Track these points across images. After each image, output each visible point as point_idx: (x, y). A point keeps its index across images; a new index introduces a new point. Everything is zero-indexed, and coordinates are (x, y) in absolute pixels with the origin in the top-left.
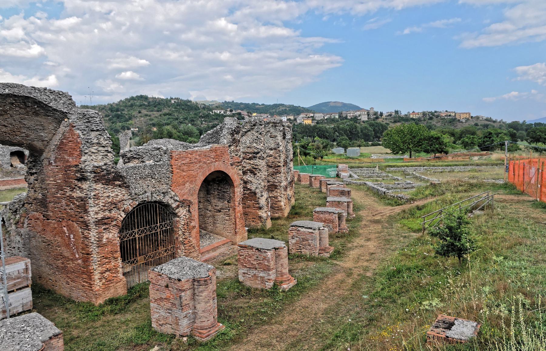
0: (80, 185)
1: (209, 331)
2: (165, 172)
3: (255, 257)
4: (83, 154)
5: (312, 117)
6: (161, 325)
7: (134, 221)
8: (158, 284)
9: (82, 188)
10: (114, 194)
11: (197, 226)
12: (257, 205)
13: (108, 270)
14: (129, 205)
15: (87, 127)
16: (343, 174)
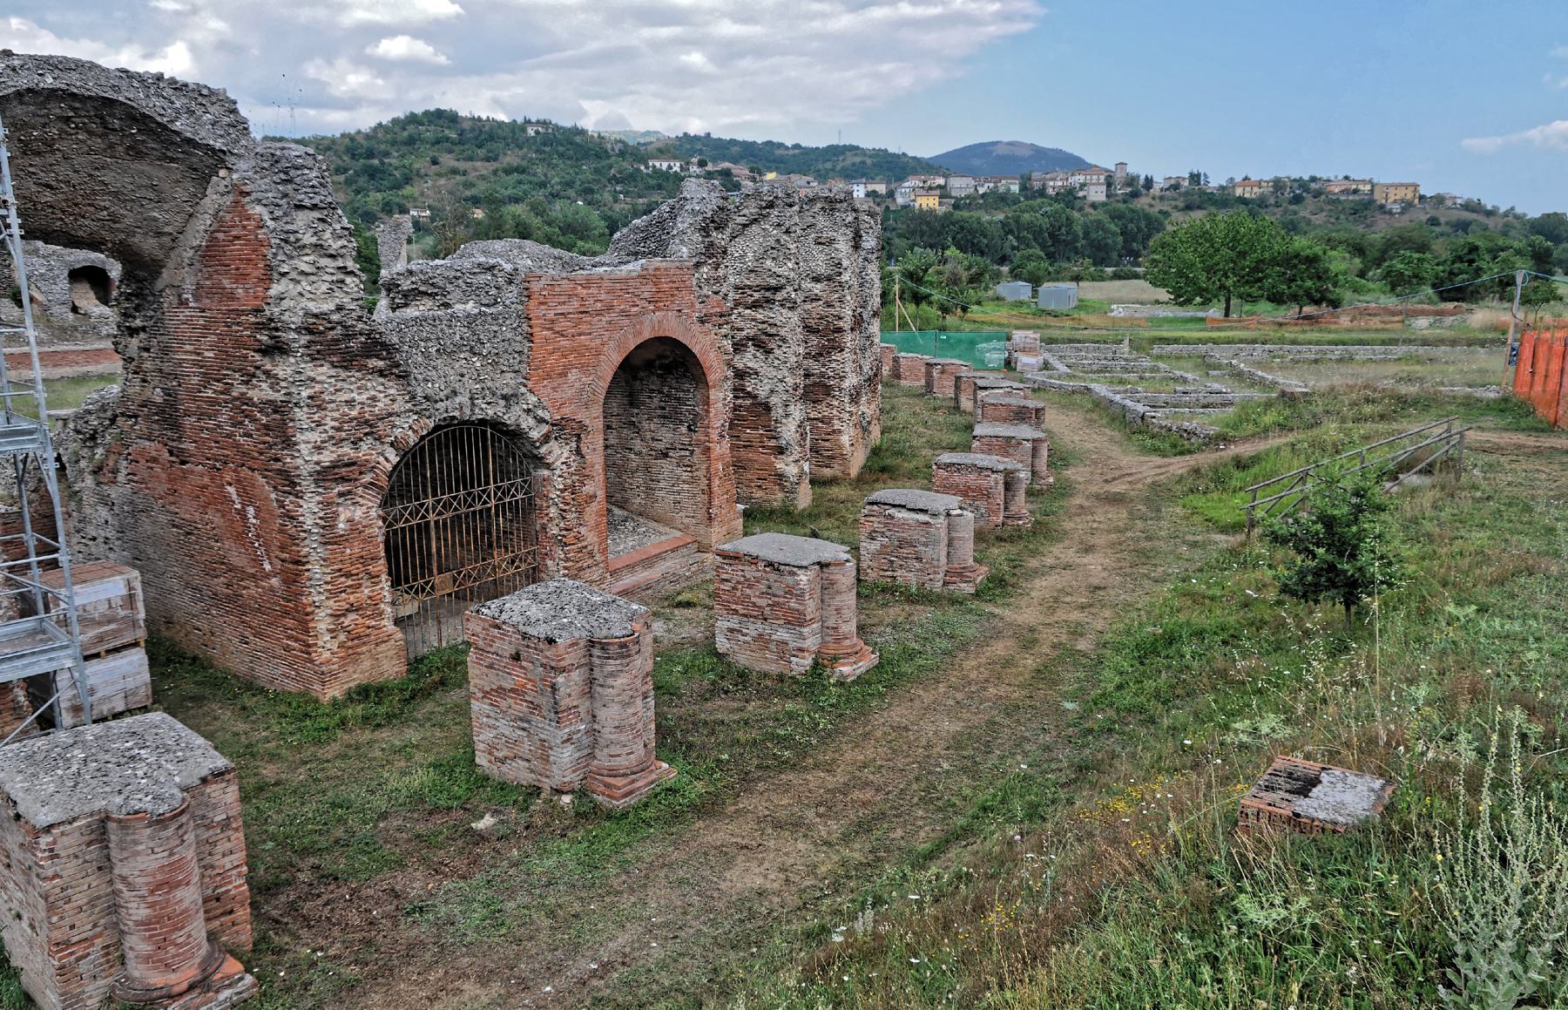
0: (268, 367)
1: (633, 781)
2: (509, 336)
3: (763, 588)
4: (276, 276)
5: (940, 187)
6: (503, 761)
7: (424, 476)
8: (492, 650)
9: (275, 377)
10: (365, 397)
11: (601, 494)
12: (773, 443)
13: (352, 609)
14: (409, 429)
15: (285, 195)
16: (1024, 360)
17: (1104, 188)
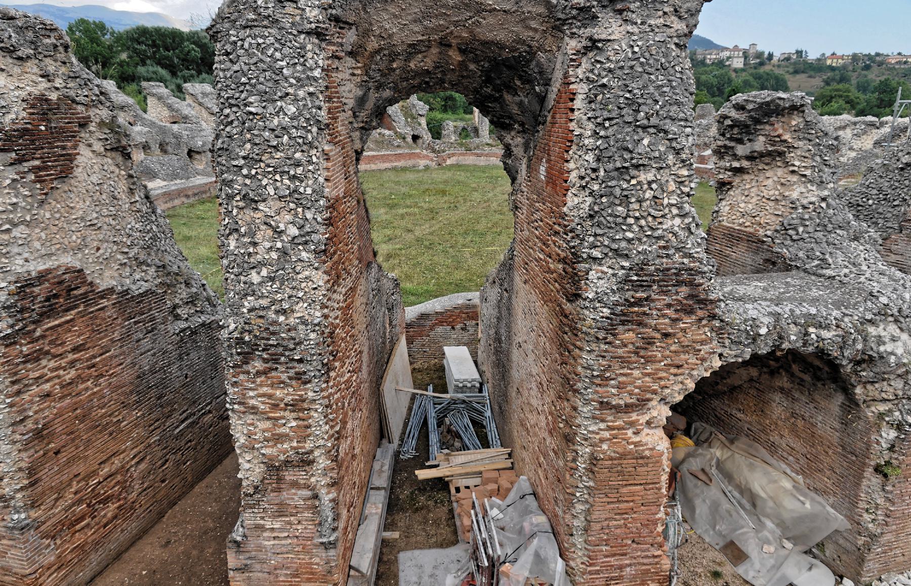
17: (742, 60)
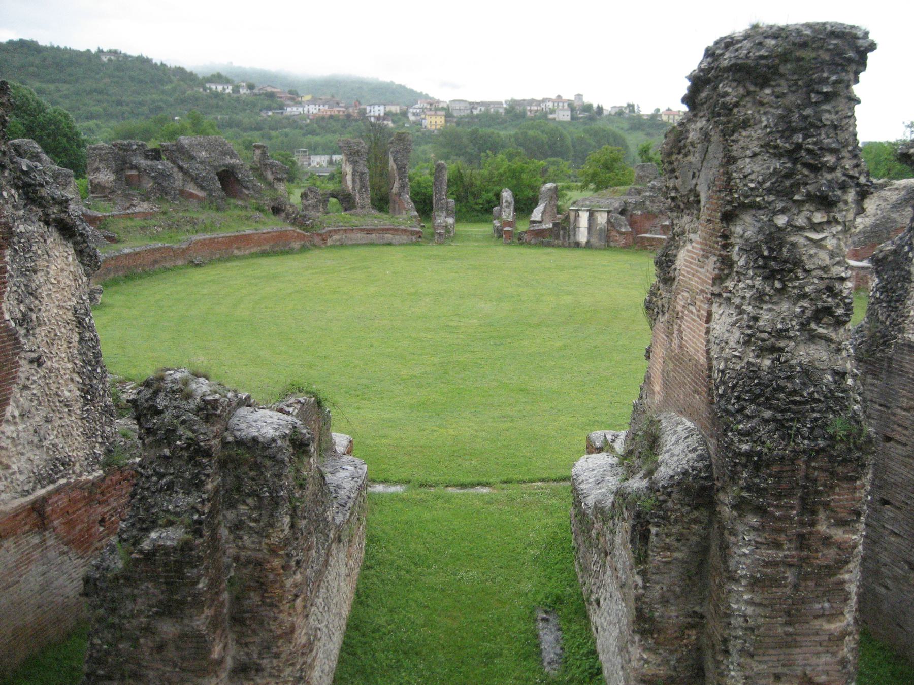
17: (569, 113)
